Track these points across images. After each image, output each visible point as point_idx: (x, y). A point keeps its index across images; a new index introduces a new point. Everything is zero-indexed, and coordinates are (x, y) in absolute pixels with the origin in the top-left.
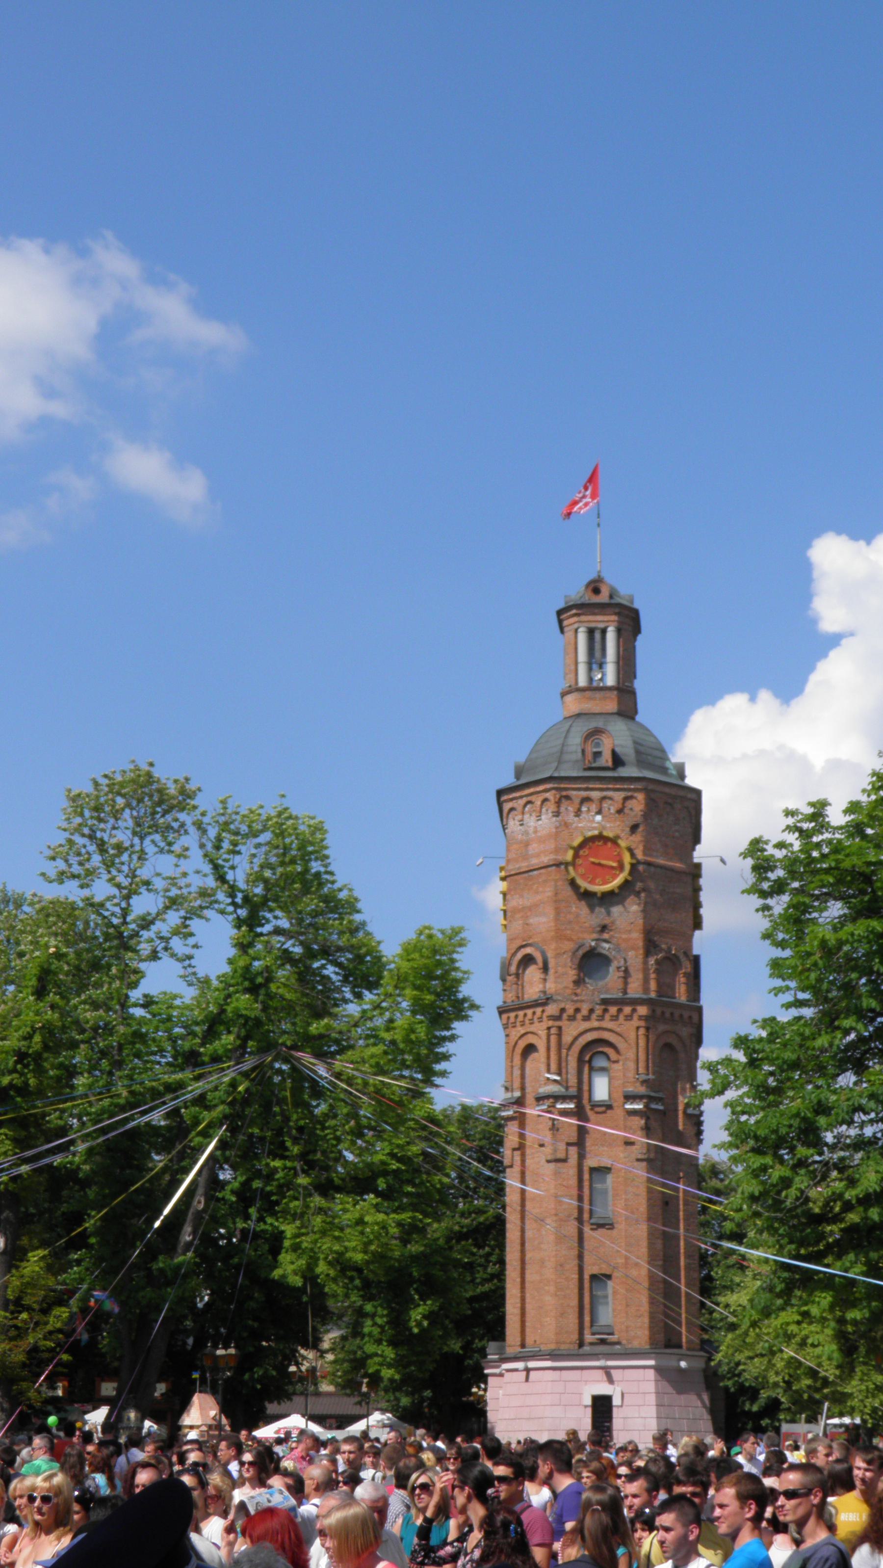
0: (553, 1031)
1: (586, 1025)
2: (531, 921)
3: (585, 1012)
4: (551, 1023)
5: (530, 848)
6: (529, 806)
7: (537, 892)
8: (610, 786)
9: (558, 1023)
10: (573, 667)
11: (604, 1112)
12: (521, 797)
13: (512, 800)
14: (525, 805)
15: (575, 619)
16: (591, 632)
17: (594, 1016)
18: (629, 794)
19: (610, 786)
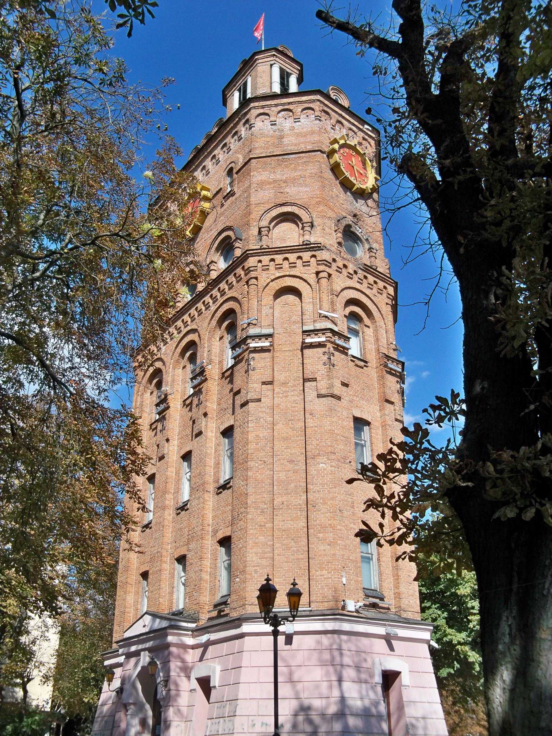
0: (321, 275)
1: (350, 283)
2: (288, 190)
3: (351, 270)
4: (321, 268)
5: (284, 140)
6: (283, 113)
7: (295, 170)
8: (356, 123)
9: (328, 269)
10: (269, 84)
11: (362, 368)
12: (276, 105)
13: (263, 107)
14: (279, 112)
15: (272, 58)
16: (282, 71)
17: (355, 278)
18: (366, 137)
19: (356, 123)
